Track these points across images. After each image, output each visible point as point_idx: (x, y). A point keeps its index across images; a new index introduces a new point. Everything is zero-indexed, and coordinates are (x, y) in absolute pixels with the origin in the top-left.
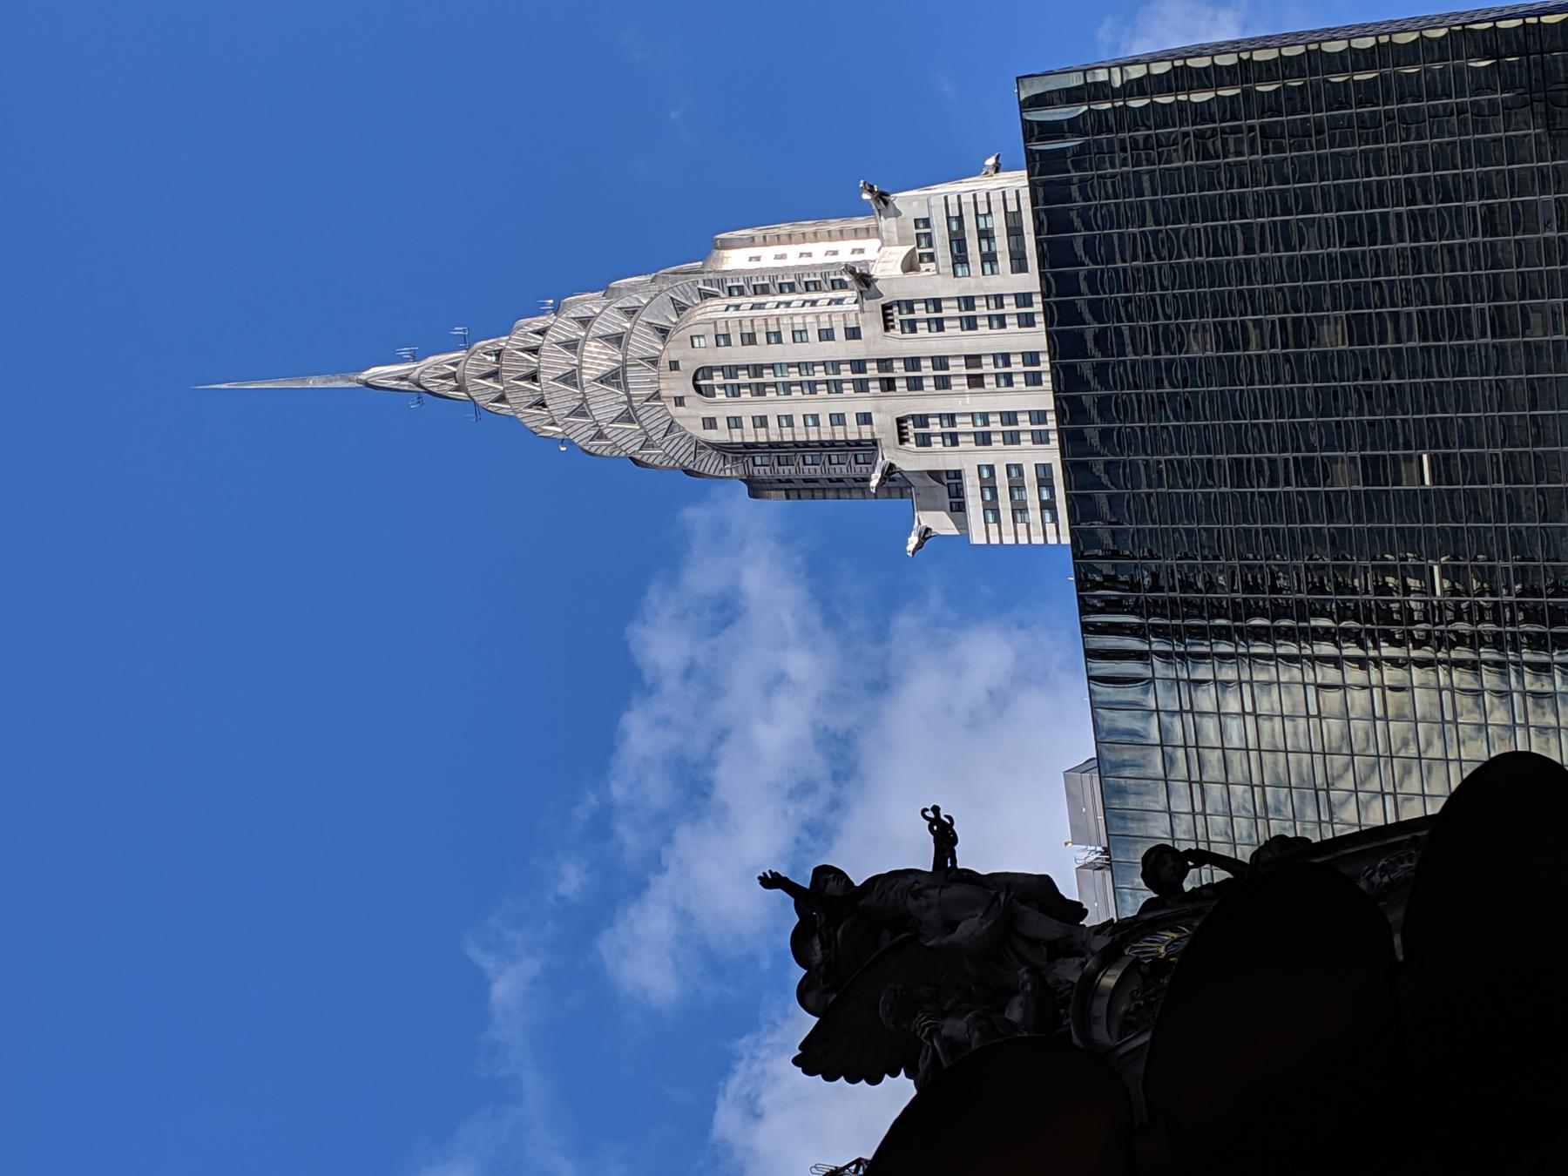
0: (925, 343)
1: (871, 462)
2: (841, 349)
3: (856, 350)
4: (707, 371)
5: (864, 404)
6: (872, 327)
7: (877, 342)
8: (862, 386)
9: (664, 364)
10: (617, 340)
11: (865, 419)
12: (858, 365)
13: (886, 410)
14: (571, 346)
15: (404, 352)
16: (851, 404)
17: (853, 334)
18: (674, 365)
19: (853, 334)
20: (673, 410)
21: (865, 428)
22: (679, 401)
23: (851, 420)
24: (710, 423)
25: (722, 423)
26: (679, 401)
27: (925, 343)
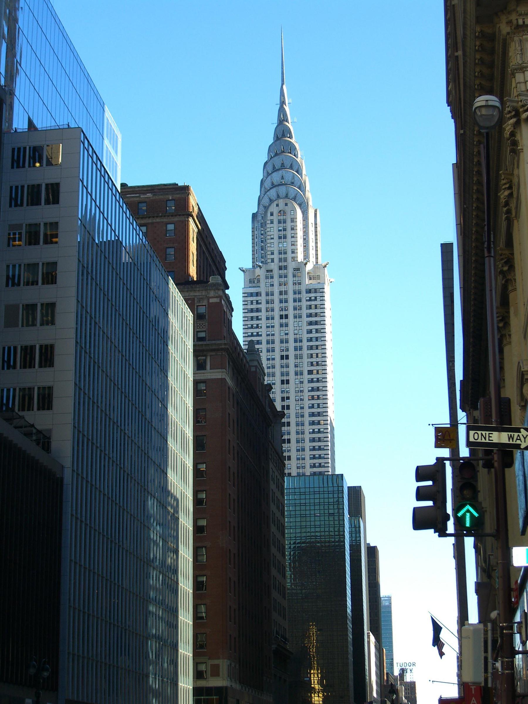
0: (290, 279)
1: (262, 262)
2: (289, 255)
3: (289, 260)
4: (285, 213)
5: (276, 260)
7: (291, 266)
8: (280, 260)
9: (287, 201)
11: (273, 260)
12: (285, 260)
13: (274, 266)
15: (290, 101)
16: (276, 257)
18: (286, 205)
20: (276, 203)
21: (270, 261)
22: (277, 205)
23: (272, 257)
24: (272, 214)
25: (272, 218)
26: (277, 205)
27: (290, 279)
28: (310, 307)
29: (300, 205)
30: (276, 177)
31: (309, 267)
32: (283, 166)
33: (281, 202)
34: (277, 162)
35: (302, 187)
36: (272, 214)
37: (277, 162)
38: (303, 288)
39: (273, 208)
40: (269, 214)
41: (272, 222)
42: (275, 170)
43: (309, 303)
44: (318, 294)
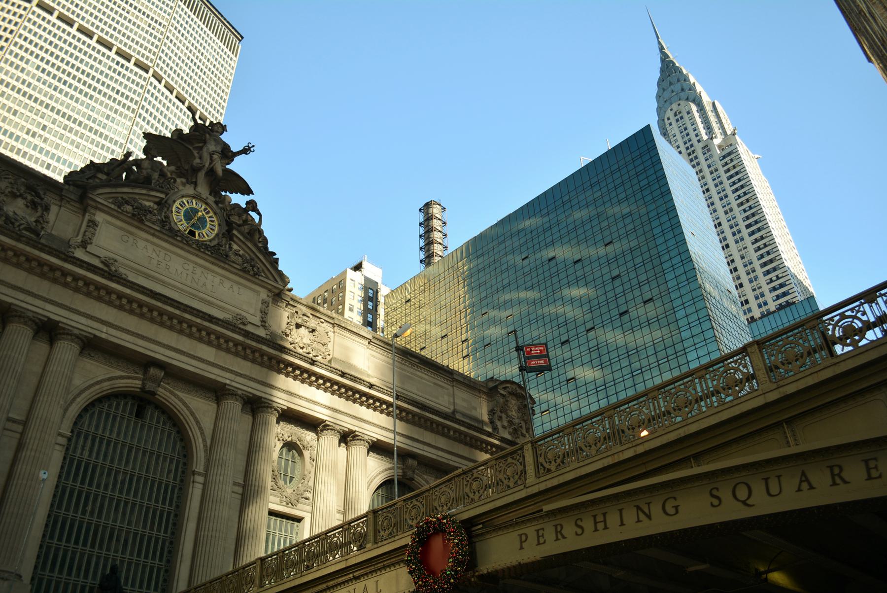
2: (695, 140)
6: (701, 145)
8: (687, 148)
10: (683, 90)
12: (692, 146)
14: (679, 80)
17: (699, 141)
19: (699, 141)
24: (669, 119)
28: (728, 170)
29: (694, 101)
30: (667, 95)
31: (717, 141)
32: (671, 84)
33: (675, 107)
34: (665, 84)
35: (692, 88)
36: (669, 119)
37: (665, 84)
38: (716, 158)
39: (670, 114)
40: (666, 120)
41: (670, 124)
42: (664, 90)
43: (726, 168)
44: (732, 156)
